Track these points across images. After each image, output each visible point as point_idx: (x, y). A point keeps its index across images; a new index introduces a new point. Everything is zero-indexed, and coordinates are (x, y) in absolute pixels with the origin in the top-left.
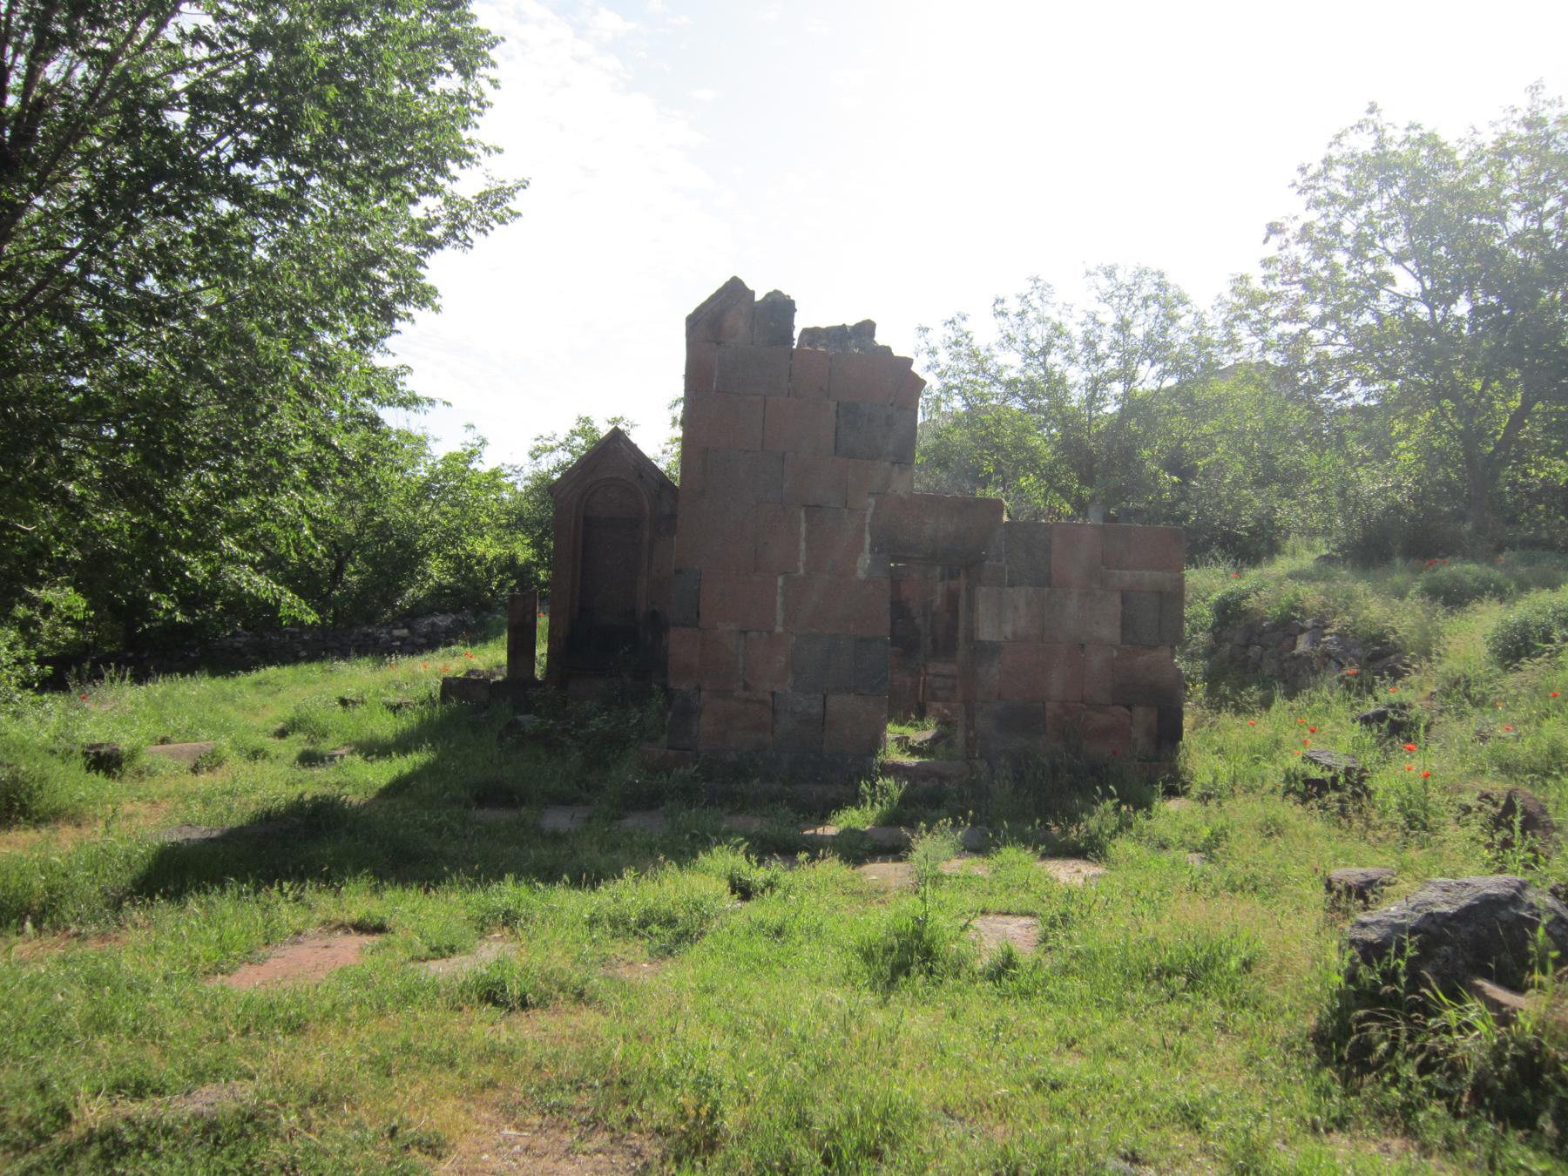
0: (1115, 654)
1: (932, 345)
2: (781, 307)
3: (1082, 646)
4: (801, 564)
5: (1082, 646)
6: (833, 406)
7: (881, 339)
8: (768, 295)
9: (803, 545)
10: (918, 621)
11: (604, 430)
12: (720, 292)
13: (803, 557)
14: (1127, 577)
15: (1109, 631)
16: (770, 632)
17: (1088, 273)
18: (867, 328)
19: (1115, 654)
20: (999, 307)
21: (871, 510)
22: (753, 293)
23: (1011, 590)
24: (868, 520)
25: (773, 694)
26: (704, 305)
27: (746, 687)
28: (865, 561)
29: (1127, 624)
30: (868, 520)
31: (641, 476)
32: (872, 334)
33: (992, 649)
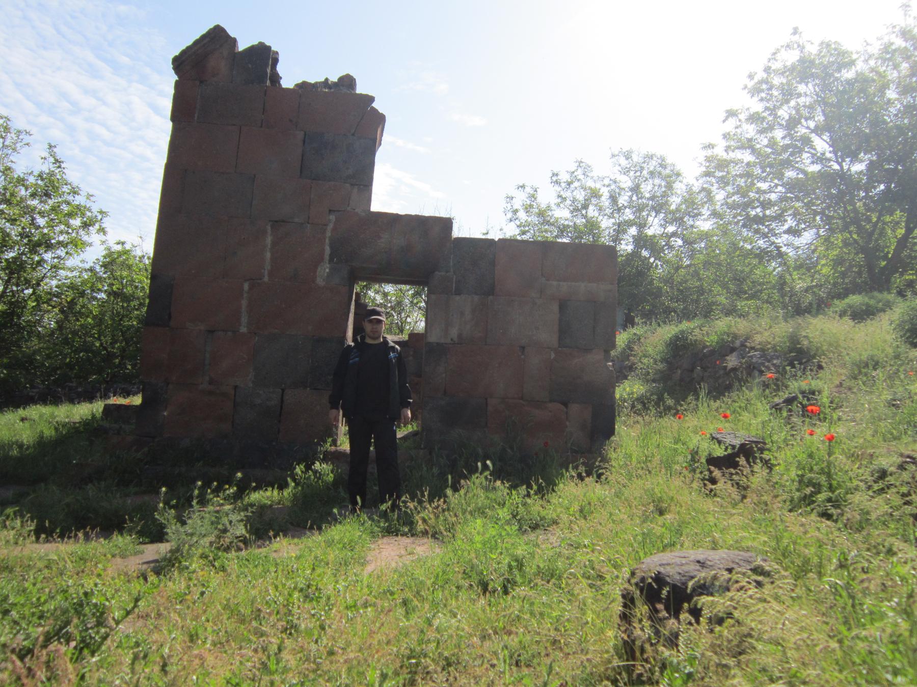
0: (553, 356)
1: (515, 208)
3: (523, 348)
5: (523, 348)
6: (300, 135)
9: (268, 255)
12: (203, 37)
15: (548, 336)
17: (613, 156)
18: (348, 82)
19: (553, 356)
20: (554, 179)
21: (331, 226)
22: (234, 41)
23: (458, 298)
24: (328, 234)
26: (188, 48)
28: (325, 269)
29: (564, 331)
30: (328, 234)
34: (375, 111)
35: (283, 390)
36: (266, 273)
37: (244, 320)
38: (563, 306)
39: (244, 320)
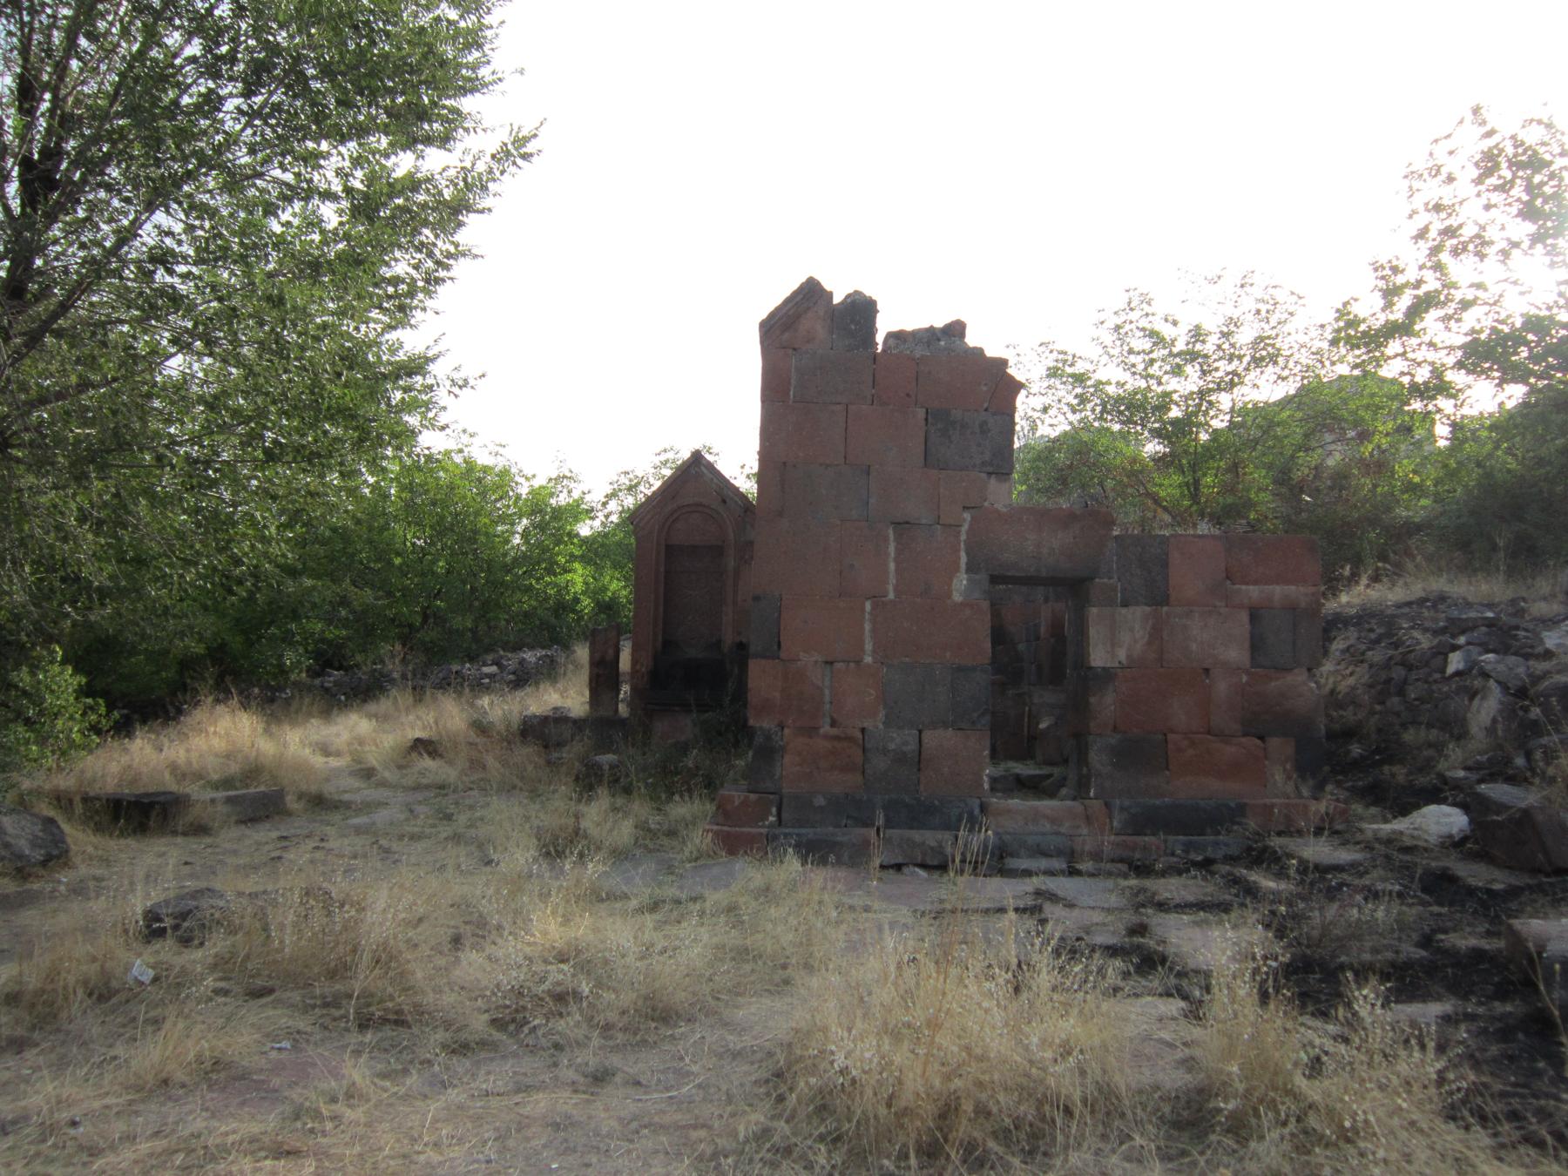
0: (1245, 678)
2: (861, 310)
3: (1207, 671)
4: (891, 588)
6: (921, 413)
7: (972, 340)
8: (848, 296)
9: (892, 566)
10: (1021, 647)
11: (685, 455)
13: (892, 580)
14: (1254, 592)
15: (1236, 654)
16: (858, 662)
18: (956, 330)
19: (1245, 678)
21: (965, 527)
22: (830, 295)
23: (1124, 611)
24: (963, 537)
25: (863, 730)
26: (778, 309)
27: (833, 724)
28: (961, 581)
31: (724, 501)
32: (962, 335)
33: (1107, 675)
34: (1011, 378)
35: (920, 732)
36: (891, 588)
37: (869, 647)
38: (1255, 615)
39: (869, 647)
